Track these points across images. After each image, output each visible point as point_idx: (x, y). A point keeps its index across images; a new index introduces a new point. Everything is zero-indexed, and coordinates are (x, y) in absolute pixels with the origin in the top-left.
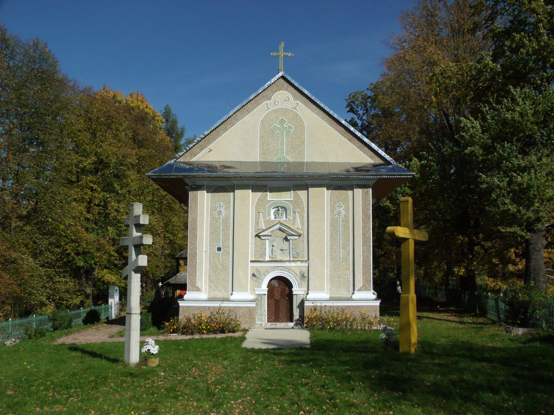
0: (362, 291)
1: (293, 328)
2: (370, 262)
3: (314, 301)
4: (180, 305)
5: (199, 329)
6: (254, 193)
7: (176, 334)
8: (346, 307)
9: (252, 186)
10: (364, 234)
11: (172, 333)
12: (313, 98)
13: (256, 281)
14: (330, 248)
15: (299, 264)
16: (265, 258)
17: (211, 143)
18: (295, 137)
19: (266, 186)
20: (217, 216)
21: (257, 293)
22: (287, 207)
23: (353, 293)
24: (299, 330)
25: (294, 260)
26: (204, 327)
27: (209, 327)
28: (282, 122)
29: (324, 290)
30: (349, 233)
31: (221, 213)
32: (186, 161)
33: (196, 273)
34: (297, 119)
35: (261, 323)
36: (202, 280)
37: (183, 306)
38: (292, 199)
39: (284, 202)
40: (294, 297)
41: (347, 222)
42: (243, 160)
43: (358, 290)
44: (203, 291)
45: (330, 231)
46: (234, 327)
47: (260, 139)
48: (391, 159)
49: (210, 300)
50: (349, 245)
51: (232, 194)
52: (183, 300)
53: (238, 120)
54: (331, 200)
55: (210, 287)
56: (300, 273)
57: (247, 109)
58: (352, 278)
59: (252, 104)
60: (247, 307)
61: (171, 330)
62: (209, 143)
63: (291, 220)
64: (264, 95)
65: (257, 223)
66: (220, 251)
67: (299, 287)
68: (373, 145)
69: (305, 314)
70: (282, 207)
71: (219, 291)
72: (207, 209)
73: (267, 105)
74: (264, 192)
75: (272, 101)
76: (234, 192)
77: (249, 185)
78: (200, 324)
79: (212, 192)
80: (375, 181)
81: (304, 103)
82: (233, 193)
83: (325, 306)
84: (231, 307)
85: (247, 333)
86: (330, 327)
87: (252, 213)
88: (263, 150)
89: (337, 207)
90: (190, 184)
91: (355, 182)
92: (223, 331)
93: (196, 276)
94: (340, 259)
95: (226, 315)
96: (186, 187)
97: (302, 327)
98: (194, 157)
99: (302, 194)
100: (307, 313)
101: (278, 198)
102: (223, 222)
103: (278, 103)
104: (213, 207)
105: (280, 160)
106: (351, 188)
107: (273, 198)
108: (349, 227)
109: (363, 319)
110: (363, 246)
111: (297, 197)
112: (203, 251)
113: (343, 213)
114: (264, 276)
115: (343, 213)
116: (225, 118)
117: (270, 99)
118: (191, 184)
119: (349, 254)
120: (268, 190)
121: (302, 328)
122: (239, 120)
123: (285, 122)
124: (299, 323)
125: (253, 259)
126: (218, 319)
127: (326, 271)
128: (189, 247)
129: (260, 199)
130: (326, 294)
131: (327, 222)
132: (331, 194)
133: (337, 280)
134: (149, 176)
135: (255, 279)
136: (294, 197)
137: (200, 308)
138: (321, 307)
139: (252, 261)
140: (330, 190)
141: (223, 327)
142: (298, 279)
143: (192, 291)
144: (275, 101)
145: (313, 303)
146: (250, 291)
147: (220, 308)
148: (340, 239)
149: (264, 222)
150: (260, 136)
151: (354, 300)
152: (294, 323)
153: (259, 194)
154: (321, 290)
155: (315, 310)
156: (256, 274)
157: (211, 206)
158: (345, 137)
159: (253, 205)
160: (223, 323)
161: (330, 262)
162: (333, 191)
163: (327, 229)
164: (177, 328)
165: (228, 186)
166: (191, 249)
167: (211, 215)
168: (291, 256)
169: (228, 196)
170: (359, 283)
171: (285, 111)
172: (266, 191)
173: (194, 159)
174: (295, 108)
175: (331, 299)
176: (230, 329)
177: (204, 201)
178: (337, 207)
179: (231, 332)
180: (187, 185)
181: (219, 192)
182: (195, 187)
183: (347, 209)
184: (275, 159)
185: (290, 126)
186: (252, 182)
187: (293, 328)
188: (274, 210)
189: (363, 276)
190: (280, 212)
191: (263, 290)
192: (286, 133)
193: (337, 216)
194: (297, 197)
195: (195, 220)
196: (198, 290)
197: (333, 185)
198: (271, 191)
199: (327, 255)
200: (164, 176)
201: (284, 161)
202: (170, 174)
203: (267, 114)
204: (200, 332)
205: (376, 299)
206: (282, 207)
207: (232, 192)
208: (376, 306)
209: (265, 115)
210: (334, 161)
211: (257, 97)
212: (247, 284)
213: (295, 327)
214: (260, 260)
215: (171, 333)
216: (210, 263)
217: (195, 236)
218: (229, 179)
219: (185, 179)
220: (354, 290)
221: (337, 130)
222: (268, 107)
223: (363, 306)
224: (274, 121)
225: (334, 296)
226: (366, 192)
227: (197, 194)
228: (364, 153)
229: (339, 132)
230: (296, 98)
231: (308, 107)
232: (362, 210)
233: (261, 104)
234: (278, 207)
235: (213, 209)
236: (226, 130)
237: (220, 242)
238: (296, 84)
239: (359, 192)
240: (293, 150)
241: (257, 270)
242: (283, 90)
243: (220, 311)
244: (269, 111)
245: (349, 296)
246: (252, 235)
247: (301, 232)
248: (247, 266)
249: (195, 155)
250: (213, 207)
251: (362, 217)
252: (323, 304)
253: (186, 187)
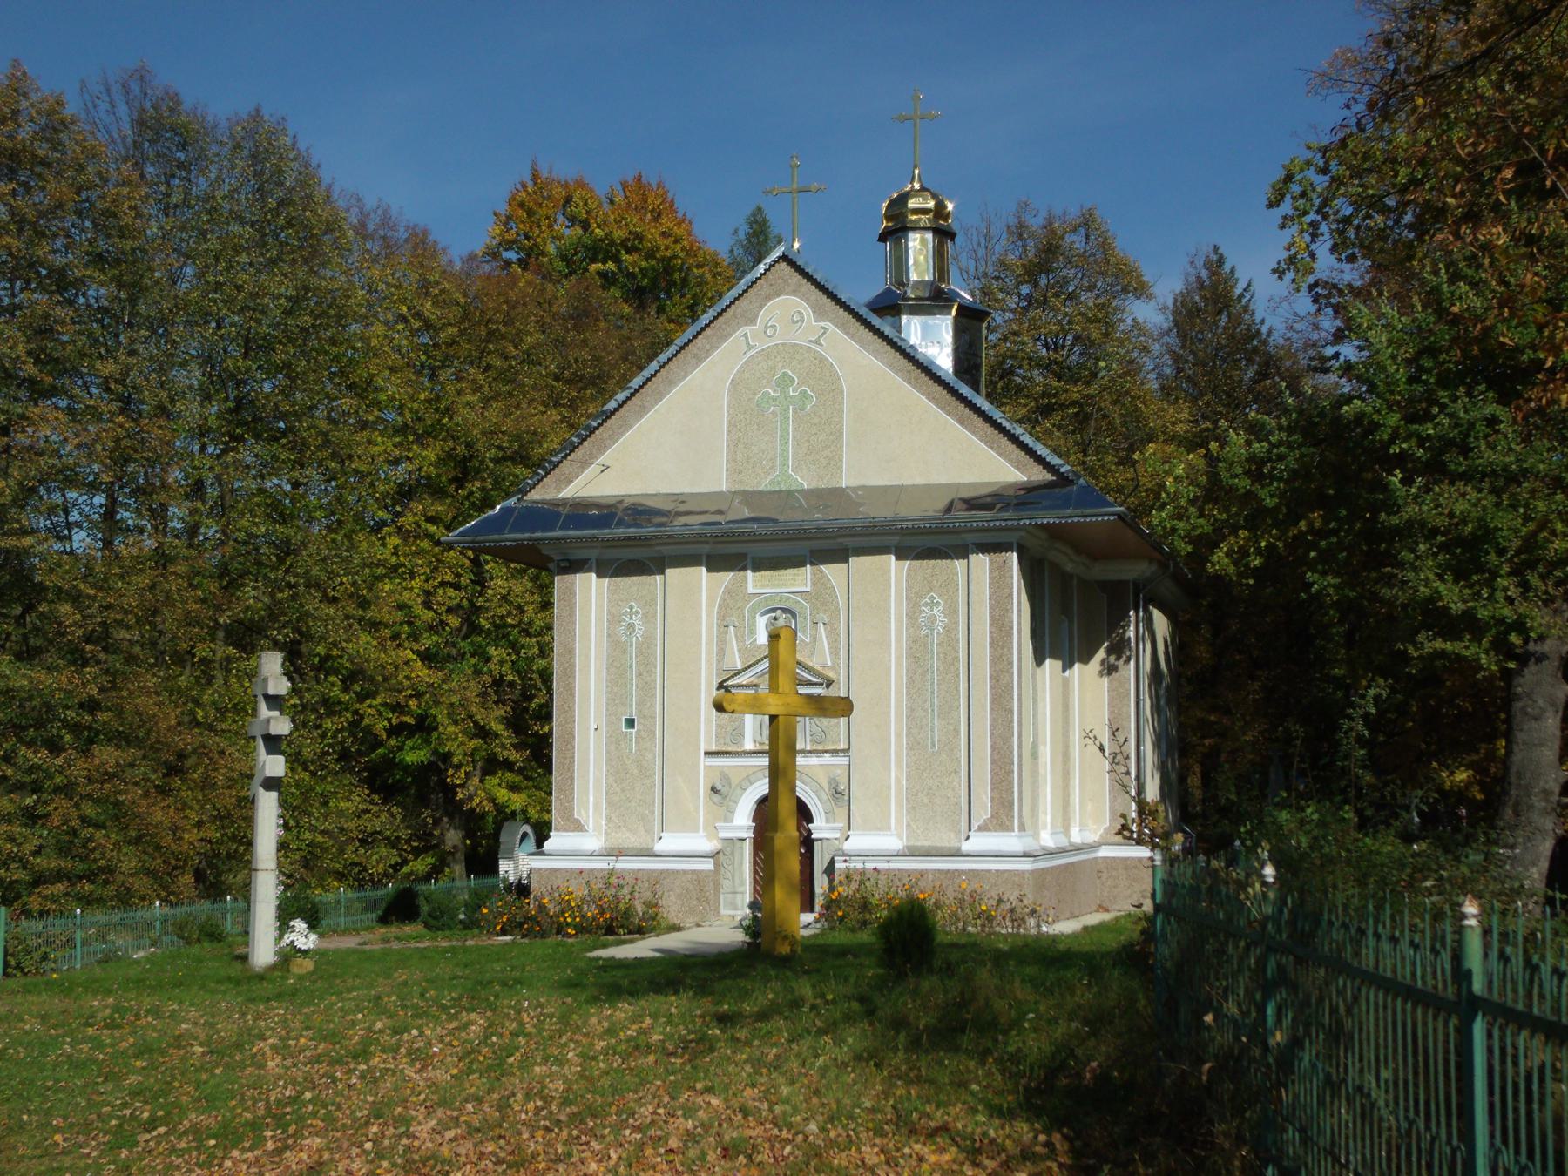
13: (721, 804)
14: (908, 717)
15: (827, 758)
16: (742, 745)
18: (816, 420)
19: (743, 556)
21: (722, 835)
22: (796, 609)
25: (815, 748)
28: (785, 381)
29: (889, 829)
30: (958, 676)
32: (548, 497)
33: (572, 784)
35: (732, 913)
38: (808, 589)
39: (788, 599)
40: (817, 845)
42: (687, 490)
43: (980, 829)
47: (729, 432)
51: (658, 578)
53: (672, 383)
54: (909, 588)
55: (609, 819)
56: (830, 783)
60: (693, 872)
62: (603, 448)
63: (807, 644)
65: (722, 653)
66: (633, 727)
67: (827, 821)
70: (784, 610)
71: (630, 830)
72: (599, 619)
73: (747, 338)
77: (700, 556)
84: (653, 871)
87: (709, 628)
90: (556, 558)
91: (970, 538)
93: (573, 793)
101: (774, 586)
102: (640, 652)
104: (613, 616)
106: (962, 552)
107: (763, 586)
110: (992, 709)
112: (588, 729)
113: (941, 621)
114: (739, 791)
117: (752, 321)
119: (957, 731)
120: (749, 565)
123: (792, 380)
125: (714, 748)
127: (896, 775)
129: (729, 592)
132: (909, 570)
133: (926, 800)
135: (716, 798)
136: (813, 584)
138: (863, 872)
139: (707, 753)
142: (825, 797)
143: (565, 830)
144: (766, 327)
146: (705, 829)
147: (612, 872)
148: (933, 693)
149: (739, 651)
150: (729, 424)
153: (727, 577)
154: (882, 827)
156: (719, 787)
159: (710, 605)
163: (899, 664)
167: (609, 636)
168: (808, 738)
171: (791, 352)
172: (744, 569)
174: (818, 342)
175: (912, 853)
183: (951, 611)
185: (805, 391)
186: (706, 548)
188: (767, 616)
189: (992, 790)
191: (739, 828)
195: (570, 651)
196: (579, 827)
198: (757, 568)
202: (496, 537)
206: (784, 610)
211: (720, 319)
212: (697, 811)
214: (729, 749)
216: (609, 760)
217: (570, 690)
219: (540, 547)
223: (988, 871)
225: (919, 844)
226: (1001, 564)
227: (574, 583)
230: (820, 314)
231: (852, 337)
233: (731, 335)
234: (774, 610)
235: (614, 620)
236: (643, 410)
237: (631, 706)
239: (981, 562)
241: (725, 777)
246: (709, 684)
247: (831, 675)
248: (696, 765)
249: (570, 482)
250: (613, 616)
252: (870, 866)
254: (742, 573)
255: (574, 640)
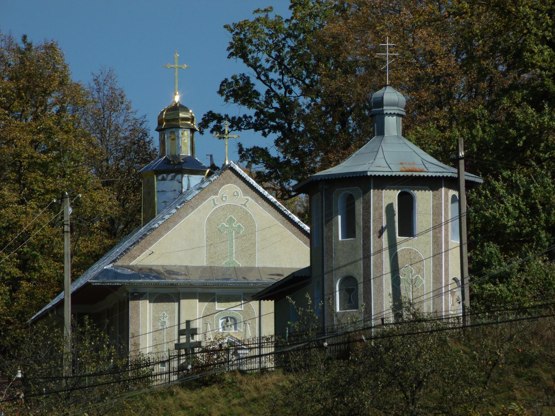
6: (201, 303)
19: (214, 294)
22: (237, 317)
28: (231, 221)
32: (125, 264)
34: (246, 216)
38: (242, 309)
47: (207, 241)
62: (150, 244)
63: (241, 332)
70: (231, 318)
72: (150, 319)
73: (214, 201)
104: (155, 318)
117: (216, 193)
123: (234, 221)
144: (222, 197)
150: (207, 237)
167: (153, 326)
171: (233, 208)
173: (133, 263)
174: (245, 205)
186: (200, 290)
190: (230, 323)
192: (235, 234)
198: (220, 301)
203: (214, 211)
221: (291, 231)
222: (214, 204)
227: (138, 304)
229: (294, 233)
230: (245, 193)
231: (259, 204)
233: (207, 199)
234: (227, 318)
240: (243, 254)
244: (217, 207)
249: (135, 258)
250: (155, 318)
255: (139, 327)
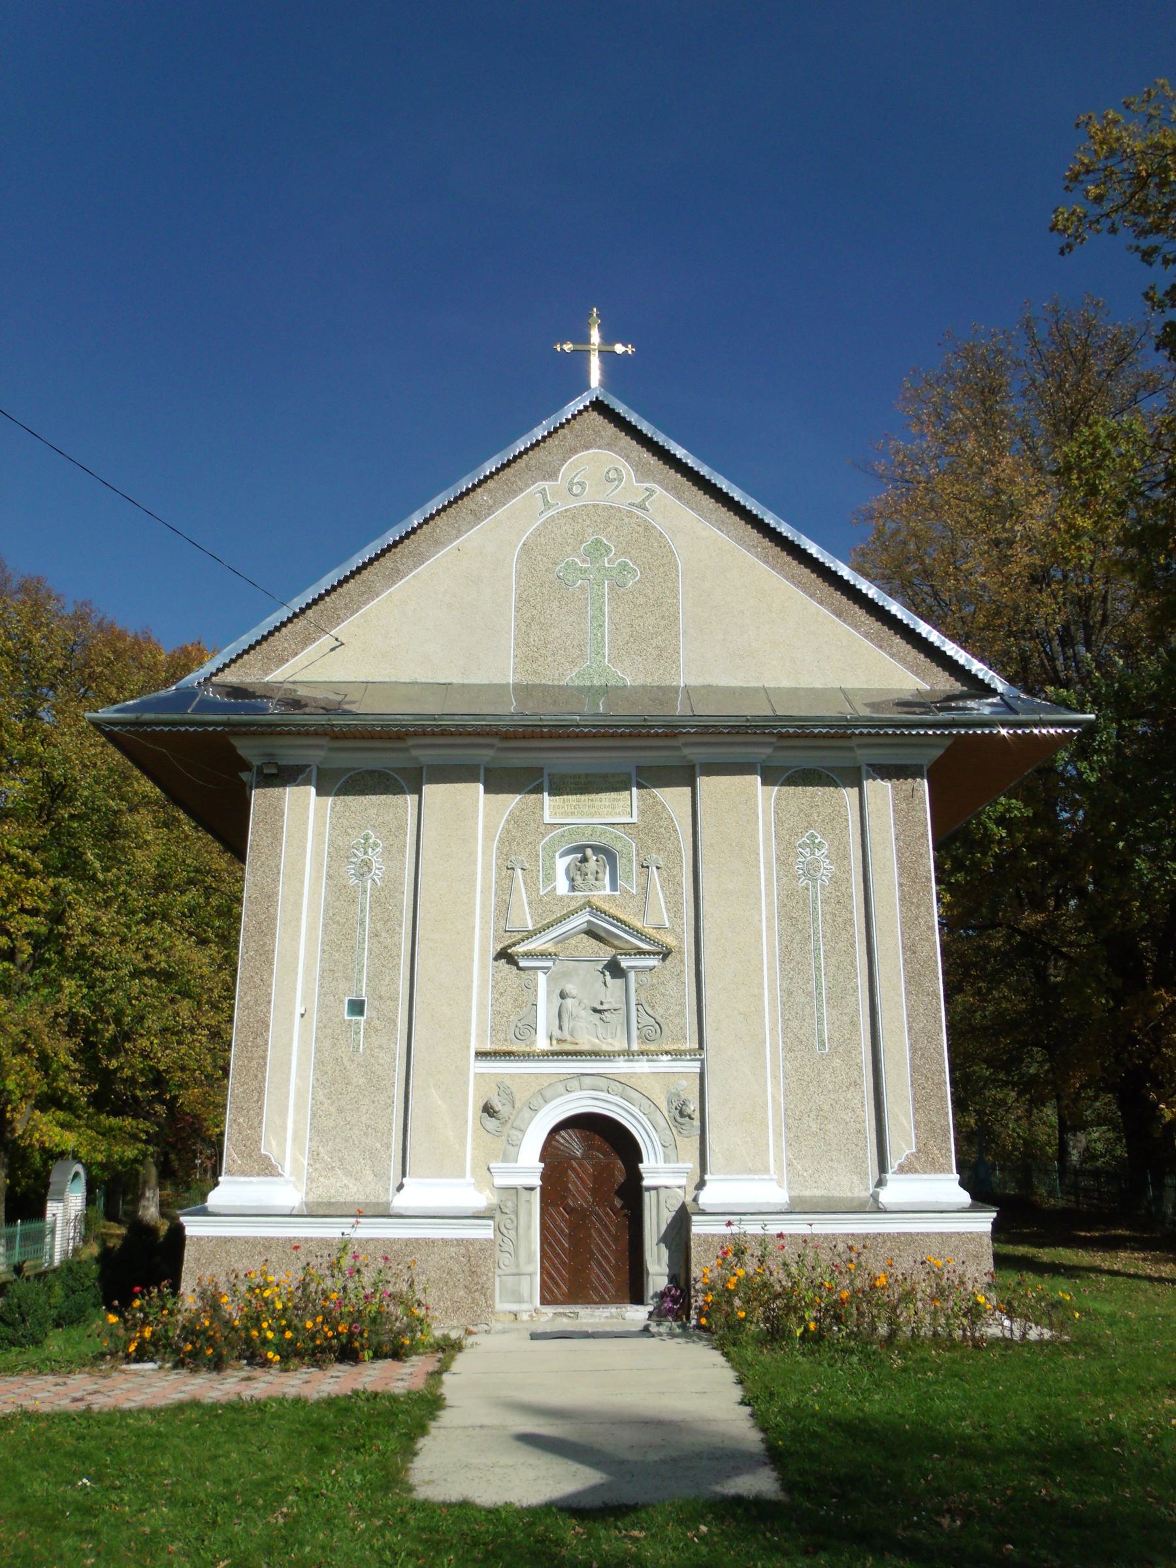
0: (916, 1171)
1: (646, 1331)
2: (941, 1055)
3: (730, 1214)
4: (189, 1231)
5: (249, 1341)
6: (492, 797)
7: (150, 1366)
8: (866, 1239)
9: (486, 769)
10: (910, 949)
11: (138, 1360)
12: (704, 471)
13: (498, 1133)
14: (783, 1004)
15: (665, 1064)
16: (533, 1043)
17: (340, 620)
18: (642, 600)
20: (353, 881)
21: (500, 1181)
22: (618, 846)
23: (880, 1183)
24: (671, 1343)
25: (644, 1047)
26: (270, 1335)
27: (289, 1335)
29: (767, 1171)
30: (853, 946)
31: (370, 870)
33: (260, 1099)
35: (514, 1307)
36: (284, 1128)
37: (200, 1239)
38: (635, 820)
39: (604, 832)
40: (649, 1199)
41: (842, 901)
42: (456, 680)
43: (902, 1169)
44: (287, 1174)
45: (780, 936)
46: (401, 1333)
47: (518, 609)
48: (991, 673)
49: (312, 1212)
50: (855, 990)
51: (411, 799)
52: (205, 1212)
53: (438, 544)
54: (779, 822)
55: (315, 1156)
56: (670, 1102)
57: (474, 507)
58: (873, 1122)
59: (490, 491)
60: (459, 1242)
61: (132, 1348)
63: (632, 896)
64: (533, 462)
65: (504, 908)
66: (361, 1013)
67: (667, 1159)
68: (924, 629)
69: (696, 1272)
70: (597, 849)
71: (348, 1174)
72: (317, 854)
74: (532, 792)
75: (561, 480)
76: (418, 791)
77: (477, 766)
78: (256, 1321)
79: (338, 794)
80: (938, 753)
81: (675, 488)
82: (416, 797)
83: (780, 1236)
84: (394, 1241)
85: (455, 1366)
86: (806, 1330)
87: (487, 869)
88: (527, 644)
89: (803, 846)
90: (256, 762)
91: (864, 756)
92: (348, 1354)
93: (259, 1114)
94: (822, 1043)
95: (368, 1277)
96: (245, 776)
97: (683, 1327)
98: (278, 667)
99: (674, 799)
100: (703, 1268)
101: (582, 814)
102: (377, 902)
103: (584, 489)
104: (338, 849)
105: (591, 679)
106: (853, 777)
107: (566, 815)
108: (849, 922)
109: (941, 1293)
110: (908, 993)
111: (653, 811)
112: (292, 1014)
113: (827, 868)
114: (527, 1113)
115: (827, 868)
116: (390, 537)
117: (552, 475)
118: (259, 763)
119: (854, 1024)
120: (546, 785)
121: (686, 1333)
122: (445, 545)
123: (608, 550)
124: (670, 1310)
125: (488, 1047)
126: (334, 1296)
127: (772, 1091)
128: (241, 999)
129: (514, 819)
130: (774, 1184)
131: (770, 904)
132: (778, 799)
133: (815, 1127)
134: (97, 725)
135: (491, 1123)
136: (642, 813)
137: (267, 1244)
138: (762, 1241)
139: (481, 1055)
140: (774, 784)
141: (351, 1335)
142: (662, 1123)
143: (244, 1173)
144: (571, 484)
145: (729, 1224)
146: (473, 1174)
147: (344, 1245)
148: (818, 969)
149: (530, 903)
150: (519, 598)
151: (886, 1212)
152: (651, 1308)
153: (513, 801)
154: (755, 1168)
155: (740, 1253)
156: (498, 1106)
157: (331, 844)
158: (821, 603)
159: (488, 838)
160: (357, 1316)
161: (785, 1058)
162: (785, 789)
163: (770, 928)
164: (155, 1341)
165: (400, 771)
166: (247, 1007)
167: (329, 877)
168: (635, 1033)
169: (396, 806)
170: (901, 1145)
171: (608, 515)
172: (538, 790)
173: (278, 675)
175: (797, 1207)
176: (380, 1345)
177: (306, 823)
178: (803, 846)
179: (386, 1357)
180: (247, 767)
181: (363, 792)
182: (274, 771)
183: (841, 856)
184: (570, 677)
185: (627, 564)
186: (485, 756)
187: (646, 1331)
188: (568, 859)
189: (916, 1110)
190: (592, 864)
191: (526, 1171)
192: (611, 589)
193: (803, 882)
194: (653, 811)
195: (270, 897)
196: (267, 1169)
197: (787, 769)
198: (557, 789)
199: (771, 1030)
200: (158, 724)
201: (603, 682)
202: (175, 717)
203: (544, 524)
204: (254, 1357)
205: (972, 1209)
206: (597, 849)
207: (412, 792)
208: (980, 1235)
209: (537, 529)
210: (786, 683)
211: (507, 470)
212: (463, 1144)
213: (654, 1328)
214: (514, 1048)
215: (128, 1359)
216: (319, 1063)
217: (266, 955)
218: (400, 745)
219: (236, 742)
220: (883, 1168)
221: (792, 578)
222: (546, 503)
223: (928, 1235)
224: (568, 549)
225: (807, 1193)
226: (909, 793)
227: (281, 799)
228: (892, 656)
229: (799, 584)
230: (643, 473)
231: (687, 504)
232: (899, 858)
233: (522, 490)
234: (581, 849)
235: (339, 854)
236: (395, 575)
237: (360, 981)
238: (645, 427)
239: (880, 791)
240: (635, 647)
241: (504, 1090)
242: (599, 448)
243: (347, 1262)
244: (552, 512)
245: (865, 1194)
246: (484, 951)
247: (670, 941)
248: (464, 1072)
249: (283, 661)
250: (338, 849)
251: (901, 885)
252: (773, 1229)
253: (245, 776)
254: (533, 796)
255: (276, 881)
